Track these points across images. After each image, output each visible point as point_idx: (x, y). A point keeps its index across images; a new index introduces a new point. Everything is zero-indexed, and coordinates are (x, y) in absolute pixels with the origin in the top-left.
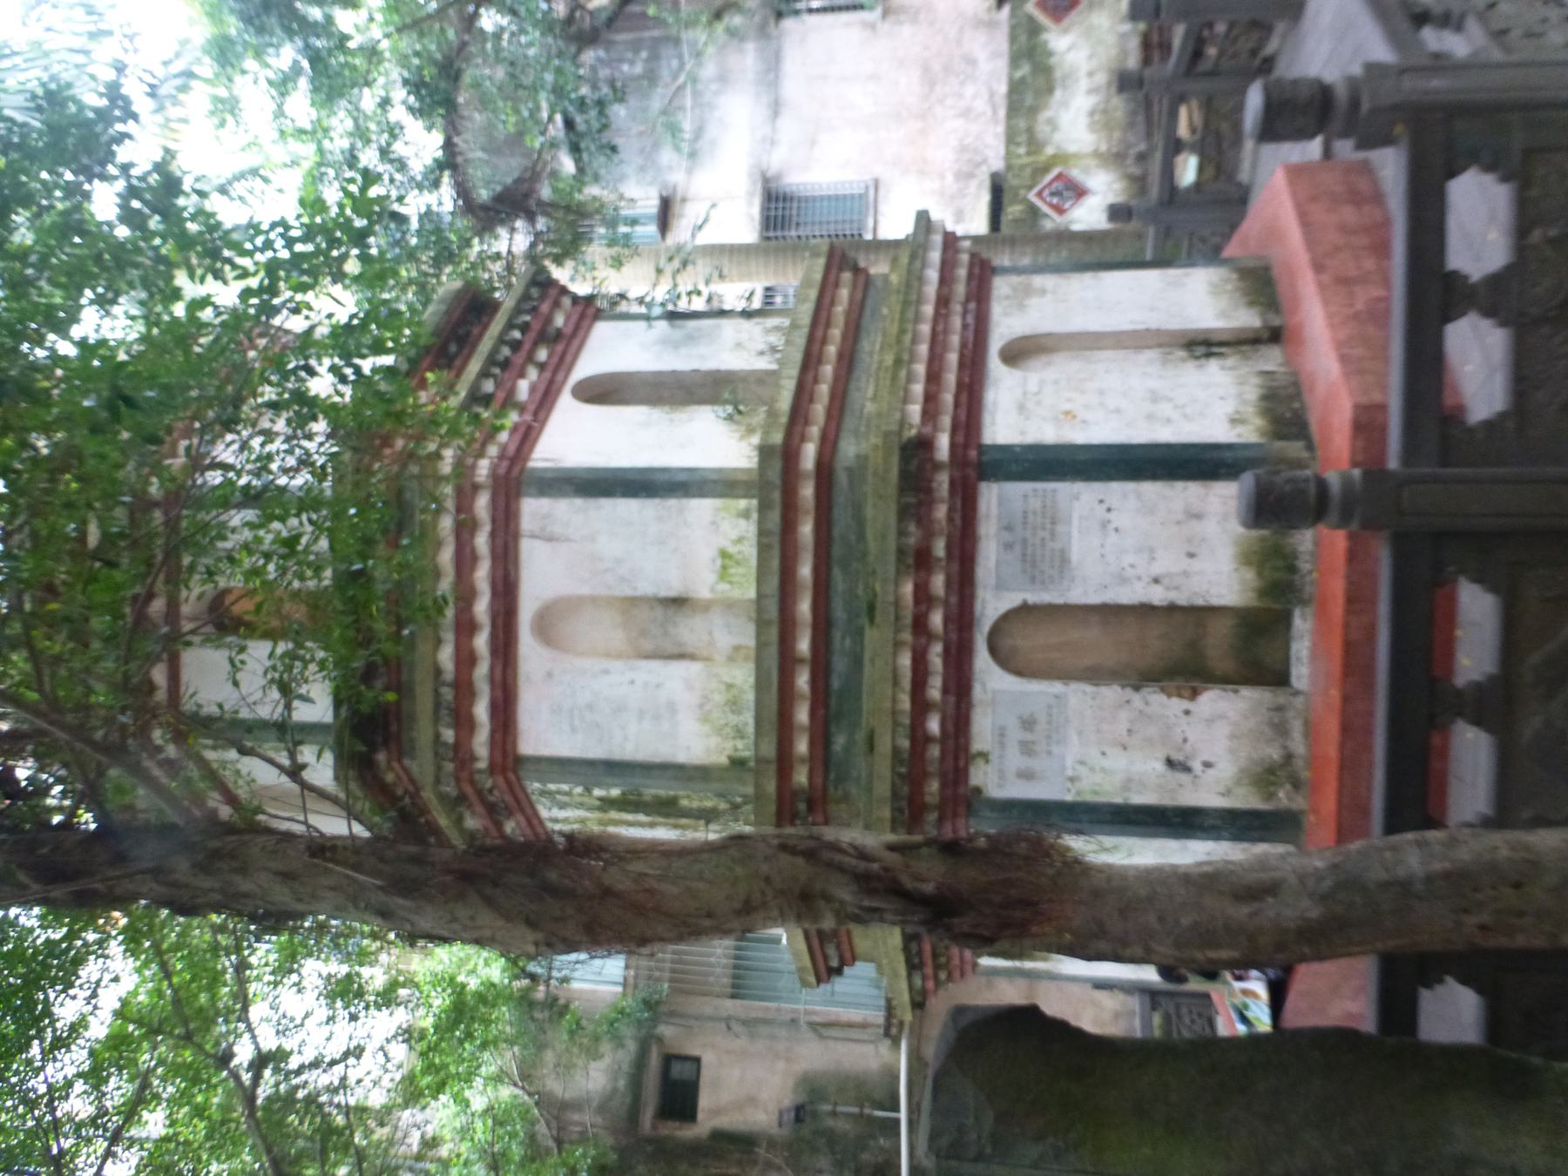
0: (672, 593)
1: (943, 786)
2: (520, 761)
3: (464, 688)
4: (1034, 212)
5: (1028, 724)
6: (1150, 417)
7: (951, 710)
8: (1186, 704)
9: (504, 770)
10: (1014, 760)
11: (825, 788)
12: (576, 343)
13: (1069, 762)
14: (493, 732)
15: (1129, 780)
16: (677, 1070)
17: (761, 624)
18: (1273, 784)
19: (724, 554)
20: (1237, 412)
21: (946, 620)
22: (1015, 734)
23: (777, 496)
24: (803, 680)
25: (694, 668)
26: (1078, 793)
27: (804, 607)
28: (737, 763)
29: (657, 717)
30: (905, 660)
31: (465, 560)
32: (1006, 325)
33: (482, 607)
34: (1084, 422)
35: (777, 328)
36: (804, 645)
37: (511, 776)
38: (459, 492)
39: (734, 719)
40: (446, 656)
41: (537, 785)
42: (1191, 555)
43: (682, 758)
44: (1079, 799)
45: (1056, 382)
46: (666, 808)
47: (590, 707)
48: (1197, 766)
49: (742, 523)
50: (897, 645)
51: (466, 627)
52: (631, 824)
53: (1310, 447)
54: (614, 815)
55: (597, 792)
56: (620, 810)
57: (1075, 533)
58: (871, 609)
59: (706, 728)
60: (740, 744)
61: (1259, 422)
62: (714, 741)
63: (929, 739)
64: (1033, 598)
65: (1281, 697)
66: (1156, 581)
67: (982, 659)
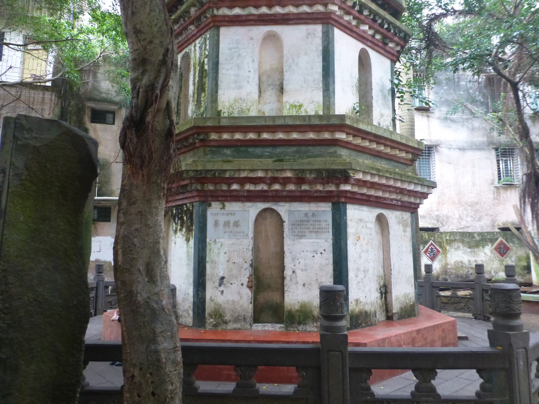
0: (285, 86)
1: (211, 191)
2: (218, 28)
4: (426, 243)
5: (236, 224)
7: (241, 194)
8: (245, 284)
9: (214, 21)
10: (222, 219)
11: (209, 146)
12: (382, 51)
13: (221, 240)
14: (229, 16)
15: (215, 263)
16: (109, 116)
18: (216, 317)
19: (301, 106)
20: (361, 302)
21: (276, 191)
22: (232, 219)
23: (325, 122)
24: (252, 136)
25: (256, 96)
26: (210, 244)
27: (281, 136)
28: (219, 113)
29: (236, 82)
30: (260, 174)
37: (211, 25)
41: (208, 36)
42: (304, 285)
43: (220, 92)
44: (207, 244)
45: (371, 234)
46: (201, 88)
47: (239, 55)
48: (222, 288)
50: (266, 171)
52: (194, 76)
54: (198, 68)
55: (206, 60)
56: (199, 70)
57: (312, 241)
58: (281, 161)
59: (232, 101)
61: (357, 310)
62: (227, 104)
63: (229, 185)
64: (286, 225)
65: (249, 320)
66: (294, 272)
67: (262, 206)
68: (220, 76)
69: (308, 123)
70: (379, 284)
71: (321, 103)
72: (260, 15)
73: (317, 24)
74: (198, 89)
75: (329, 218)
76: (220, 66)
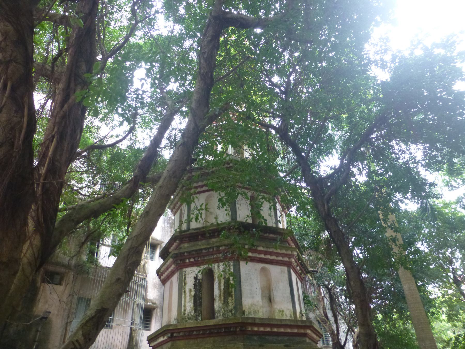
0: (272, 299)
3: (255, 251)
16: (57, 278)
17: (269, 319)
19: (283, 311)
23: (304, 324)
24: (268, 329)
27: (282, 330)
28: (243, 312)
29: (251, 294)
31: (278, 254)
33: (268, 257)
36: (275, 330)
38: (289, 255)
39: (252, 312)
40: (260, 248)
41: (232, 264)
43: (243, 299)
46: (227, 293)
47: (251, 278)
49: (289, 316)
51: (266, 253)
52: (220, 284)
54: (223, 281)
55: (231, 278)
56: (225, 283)
60: (247, 313)
62: (247, 307)
68: (242, 289)
69: (296, 324)
71: (292, 310)
72: (260, 258)
74: (224, 293)
76: (242, 284)
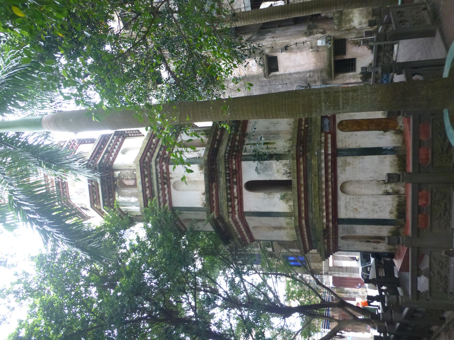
6: (373, 211)
12: (240, 172)
20: (392, 210)
32: (342, 178)
33: (243, 230)
34: (359, 212)
35: (286, 164)
45: (353, 199)
51: (241, 233)
53: (405, 221)
61: (395, 213)
70: (382, 184)
73: (245, 219)
75: (346, 226)
